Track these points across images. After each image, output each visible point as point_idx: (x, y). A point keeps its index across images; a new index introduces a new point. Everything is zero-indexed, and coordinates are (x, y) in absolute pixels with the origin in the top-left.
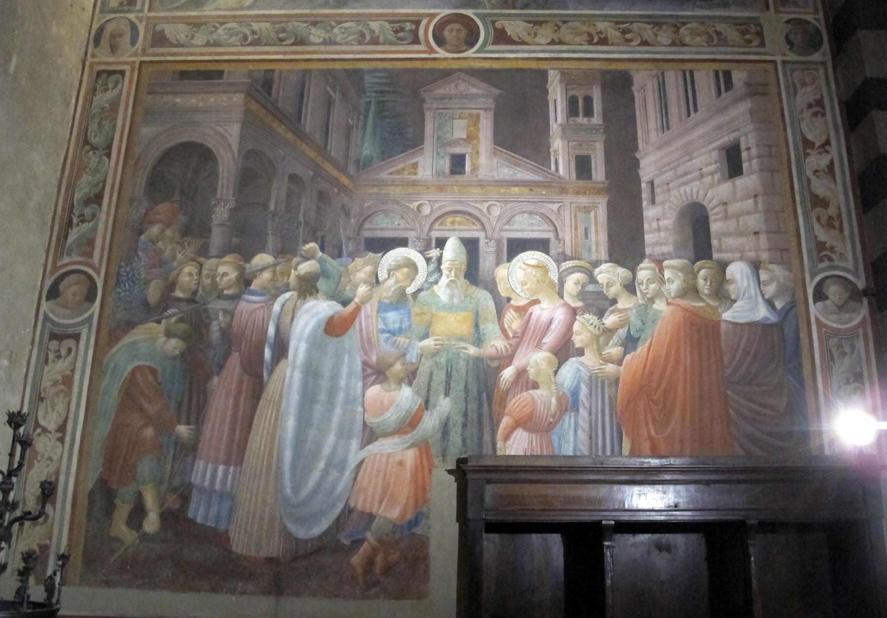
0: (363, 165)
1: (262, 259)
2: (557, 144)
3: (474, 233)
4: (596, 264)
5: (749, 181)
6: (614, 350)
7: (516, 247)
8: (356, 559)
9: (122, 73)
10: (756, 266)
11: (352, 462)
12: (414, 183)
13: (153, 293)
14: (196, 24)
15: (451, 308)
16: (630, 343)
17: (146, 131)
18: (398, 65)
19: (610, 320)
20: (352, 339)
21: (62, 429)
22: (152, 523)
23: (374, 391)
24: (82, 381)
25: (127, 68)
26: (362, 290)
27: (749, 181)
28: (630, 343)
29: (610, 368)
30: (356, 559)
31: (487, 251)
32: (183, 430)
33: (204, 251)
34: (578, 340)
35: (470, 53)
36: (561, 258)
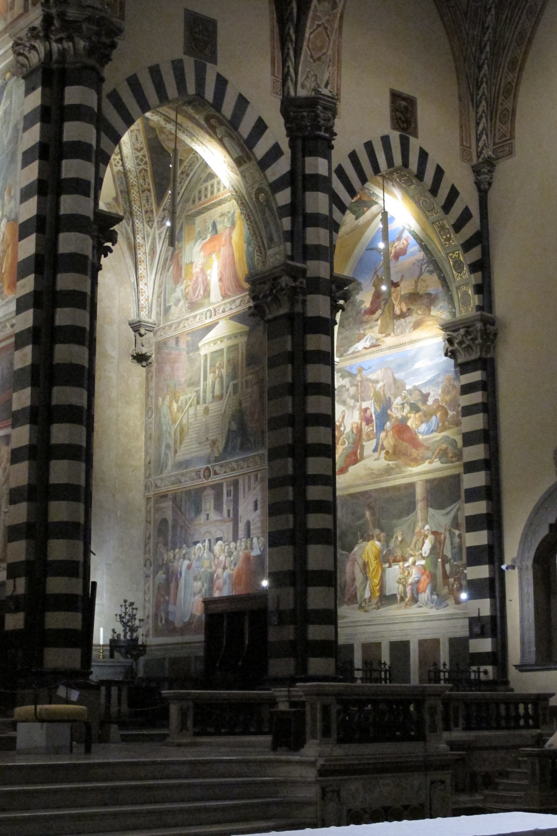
0: (192, 520)
1: (177, 550)
2: (225, 507)
3: (211, 538)
4: (230, 542)
5: (259, 512)
6: (232, 567)
7: (218, 539)
8: (193, 626)
9: (150, 498)
10: (258, 538)
11: (192, 601)
12: (200, 524)
13: (160, 562)
14: (162, 479)
15: (206, 559)
16: (235, 564)
17: (157, 516)
18: (197, 487)
19: (232, 558)
20: (191, 570)
21: (149, 600)
22: (163, 622)
23: (195, 583)
24: (151, 587)
25: (151, 496)
26: (193, 556)
27: (259, 512)
28: (235, 564)
29: (232, 572)
30: (193, 626)
31: (212, 541)
32: (167, 597)
33: (167, 550)
34: (227, 565)
35: (210, 480)
36: (224, 542)
